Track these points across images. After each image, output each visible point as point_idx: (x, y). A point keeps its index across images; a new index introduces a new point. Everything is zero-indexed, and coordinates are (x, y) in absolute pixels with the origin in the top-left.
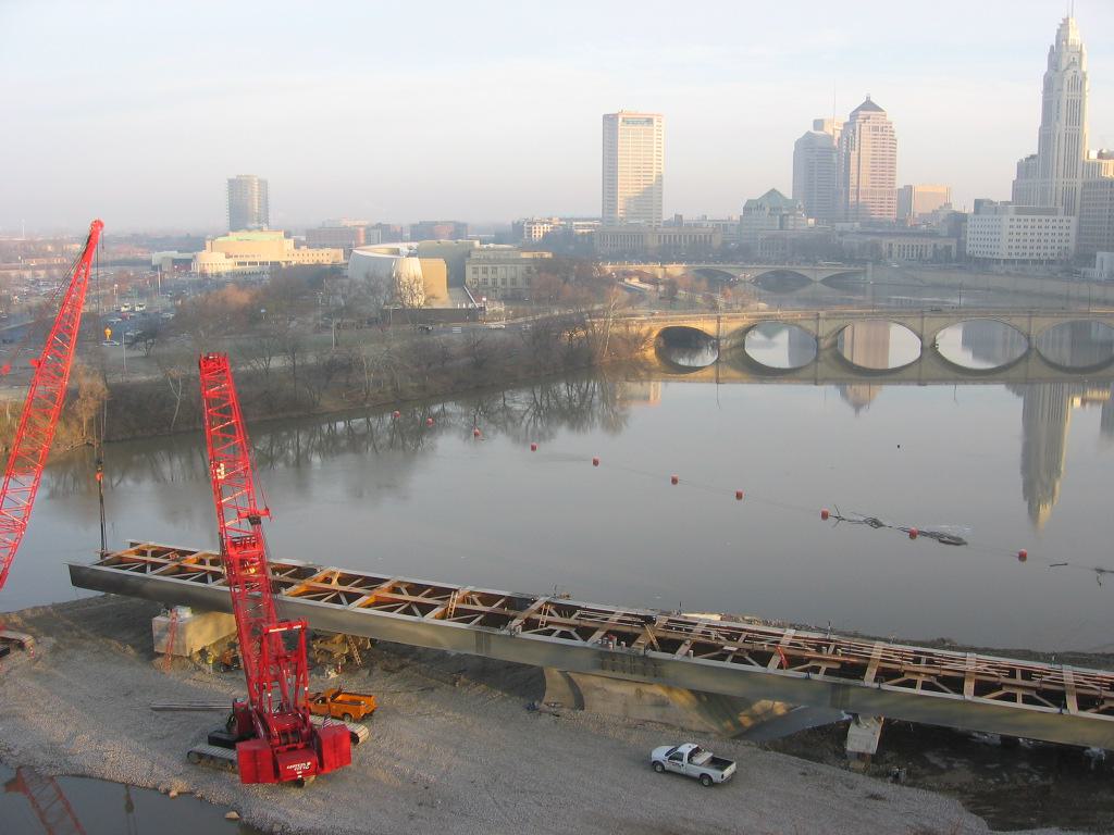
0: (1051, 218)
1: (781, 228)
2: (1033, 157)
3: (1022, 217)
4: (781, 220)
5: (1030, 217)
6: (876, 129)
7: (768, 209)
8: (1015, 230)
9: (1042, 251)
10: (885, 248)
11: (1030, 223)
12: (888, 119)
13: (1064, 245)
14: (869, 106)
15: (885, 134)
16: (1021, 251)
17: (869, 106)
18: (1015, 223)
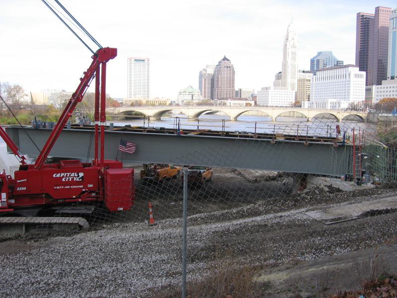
0: (286, 91)
1: (192, 98)
2: (280, 73)
3: (276, 91)
4: (192, 96)
5: (279, 91)
6: (227, 67)
7: (187, 93)
8: (273, 95)
9: (283, 103)
10: (228, 104)
11: (278, 93)
12: (232, 64)
13: (290, 101)
14: (225, 59)
15: (230, 68)
16: (276, 103)
17: (225, 59)
18: (273, 93)
